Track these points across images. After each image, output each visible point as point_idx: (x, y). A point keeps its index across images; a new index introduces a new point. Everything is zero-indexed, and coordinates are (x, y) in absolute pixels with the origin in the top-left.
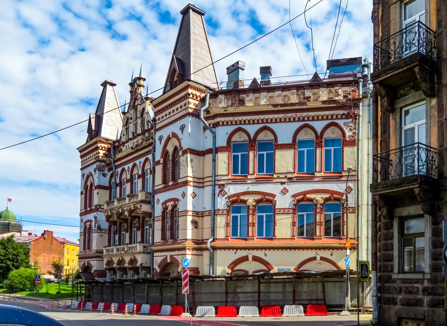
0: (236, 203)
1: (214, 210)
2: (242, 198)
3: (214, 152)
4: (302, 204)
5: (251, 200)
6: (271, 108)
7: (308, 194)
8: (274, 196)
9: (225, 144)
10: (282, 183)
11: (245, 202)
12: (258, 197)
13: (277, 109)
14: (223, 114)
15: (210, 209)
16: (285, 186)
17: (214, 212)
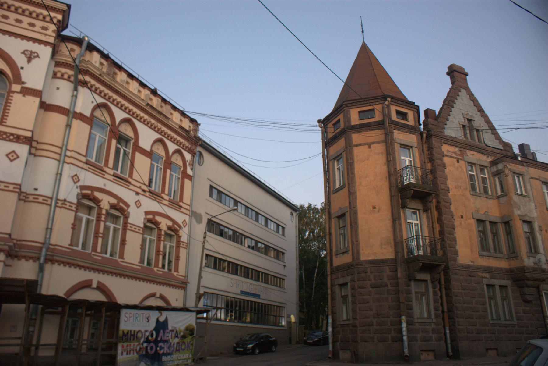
0: (88, 198)
1: (57, 199)
2: (98, 195)
3: (71, 115)
4: (151, 223)
5: (106, 201)
6: (143, 104)
7: (158, 215)
8: (128, 206)
9: (88, 113)
10: (137, 193)
11: (97, 201)
12: (114, 201)
13: (148, 109)
14: (96, 76)
15: (50, 195)
16: (140, 197)
17: (56, 203)
